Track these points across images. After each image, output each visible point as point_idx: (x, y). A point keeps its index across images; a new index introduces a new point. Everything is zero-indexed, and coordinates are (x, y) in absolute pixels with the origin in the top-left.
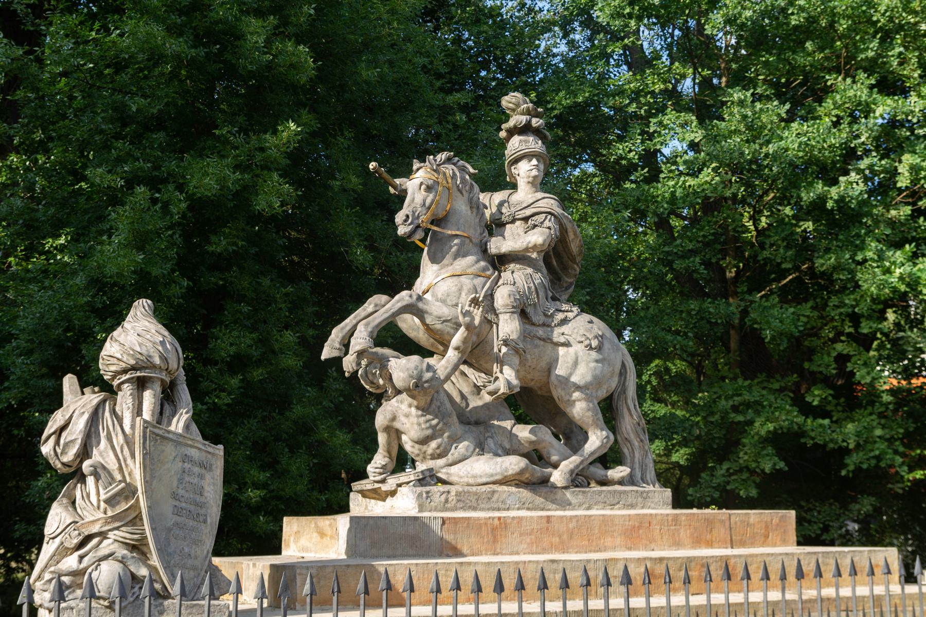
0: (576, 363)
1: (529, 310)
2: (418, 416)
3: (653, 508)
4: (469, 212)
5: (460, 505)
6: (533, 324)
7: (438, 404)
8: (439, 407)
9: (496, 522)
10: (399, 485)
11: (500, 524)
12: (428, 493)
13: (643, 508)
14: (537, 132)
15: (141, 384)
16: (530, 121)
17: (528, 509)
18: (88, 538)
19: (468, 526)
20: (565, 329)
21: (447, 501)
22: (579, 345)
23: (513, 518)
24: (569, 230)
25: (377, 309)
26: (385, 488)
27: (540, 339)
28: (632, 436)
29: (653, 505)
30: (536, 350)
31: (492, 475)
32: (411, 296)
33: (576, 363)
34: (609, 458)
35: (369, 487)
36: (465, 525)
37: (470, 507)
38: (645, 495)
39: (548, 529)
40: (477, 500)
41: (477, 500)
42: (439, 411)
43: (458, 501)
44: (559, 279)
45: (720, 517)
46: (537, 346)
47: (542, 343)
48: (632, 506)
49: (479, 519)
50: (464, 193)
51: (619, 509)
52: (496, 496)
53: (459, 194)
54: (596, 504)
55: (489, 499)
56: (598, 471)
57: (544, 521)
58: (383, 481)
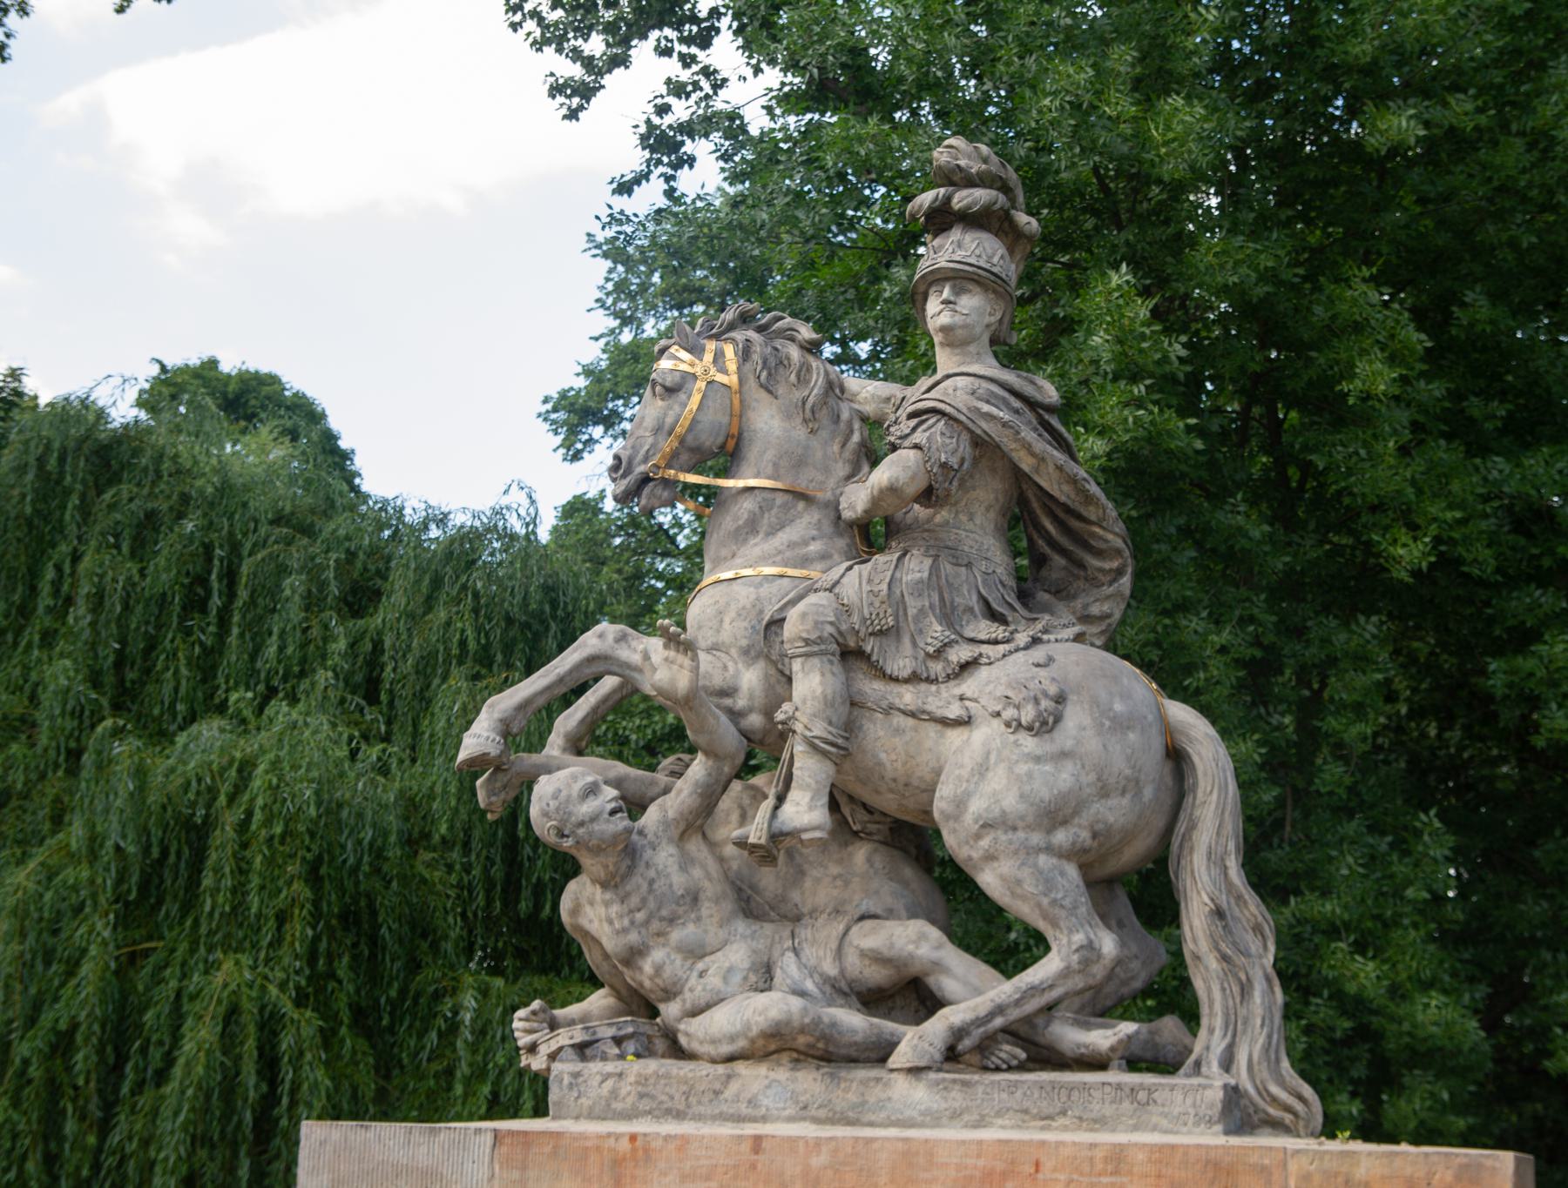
0: (982, 769)
2: (607, 904)
3: (1166, 1132)
4: (800, 433)
5: (645, 1105)
6: (895, 680)
7: (652, 873)
8: (651, 882)
9: (624, 1145)
11: (634, 1150)
12: (576, 1075)
13: (1135, 1128)
14: (974, 220)
16: (948, 199)
17: (817, 1121)
19: (555, 1153)
20: (969, 686)
21: (614, 1093)
22: (996, 722)
23: (668, 1138)
24: (1008, 444)
27: (904, 713)
28: (1204, 946)
29: (1164, 1123)
30: (897, 740)
31: (732, 1039)
32: (622, 638)
33: (982, 769)
36: (548, 1149)
37: (668, 1112)
38: (1142, 1096)
39: (753, 1166)
40: (687, 1095)
41: (687, 1095)
42: (651, 891)
43: (642, 1096)
44: (1081, 565)
45: (1254, 1159)
46: (898, 731)
47: (910, 722)
48: (1100, 1123)
49: (583, 1136)
50: (781, 391)
51: (1065, 1128)
52: (734, 1087)
53: (763, 394)
54: (999, 1114)
55: (717, 1093)
57: (746, 1147)
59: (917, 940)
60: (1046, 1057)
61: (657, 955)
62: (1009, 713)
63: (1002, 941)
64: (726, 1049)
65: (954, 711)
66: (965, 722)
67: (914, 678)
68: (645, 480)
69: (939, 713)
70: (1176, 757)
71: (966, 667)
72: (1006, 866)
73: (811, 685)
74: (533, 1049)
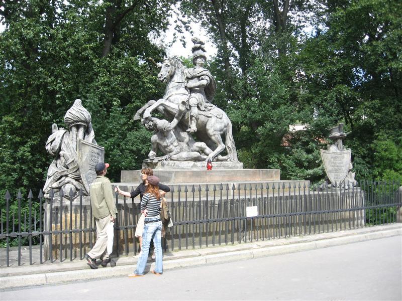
1: (200, 106)
6: (201, 110)
10: (159, 161)
15: (78, 127)
18: (61, 177)
24: (213, 81)
25: (155, 104)
26: (154, 161)
34: (224, 153)
35: (149, 161)
56: (220, 157)
58: (153, 160)
59: (202, 144)
60: (218, 160)
61: (171, 147)
62: (218, 116)
63: (212, 145)
64: (186, 159)
65: (210, 115)
66: (211, 117)
67: (204, 111)
68: (165, 78)
69: (208, 115)
70: (228, 124)
71: (210, 109)
72: (216, 136)
73: (195, 111)
74: (153, 160)
